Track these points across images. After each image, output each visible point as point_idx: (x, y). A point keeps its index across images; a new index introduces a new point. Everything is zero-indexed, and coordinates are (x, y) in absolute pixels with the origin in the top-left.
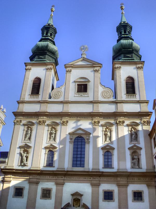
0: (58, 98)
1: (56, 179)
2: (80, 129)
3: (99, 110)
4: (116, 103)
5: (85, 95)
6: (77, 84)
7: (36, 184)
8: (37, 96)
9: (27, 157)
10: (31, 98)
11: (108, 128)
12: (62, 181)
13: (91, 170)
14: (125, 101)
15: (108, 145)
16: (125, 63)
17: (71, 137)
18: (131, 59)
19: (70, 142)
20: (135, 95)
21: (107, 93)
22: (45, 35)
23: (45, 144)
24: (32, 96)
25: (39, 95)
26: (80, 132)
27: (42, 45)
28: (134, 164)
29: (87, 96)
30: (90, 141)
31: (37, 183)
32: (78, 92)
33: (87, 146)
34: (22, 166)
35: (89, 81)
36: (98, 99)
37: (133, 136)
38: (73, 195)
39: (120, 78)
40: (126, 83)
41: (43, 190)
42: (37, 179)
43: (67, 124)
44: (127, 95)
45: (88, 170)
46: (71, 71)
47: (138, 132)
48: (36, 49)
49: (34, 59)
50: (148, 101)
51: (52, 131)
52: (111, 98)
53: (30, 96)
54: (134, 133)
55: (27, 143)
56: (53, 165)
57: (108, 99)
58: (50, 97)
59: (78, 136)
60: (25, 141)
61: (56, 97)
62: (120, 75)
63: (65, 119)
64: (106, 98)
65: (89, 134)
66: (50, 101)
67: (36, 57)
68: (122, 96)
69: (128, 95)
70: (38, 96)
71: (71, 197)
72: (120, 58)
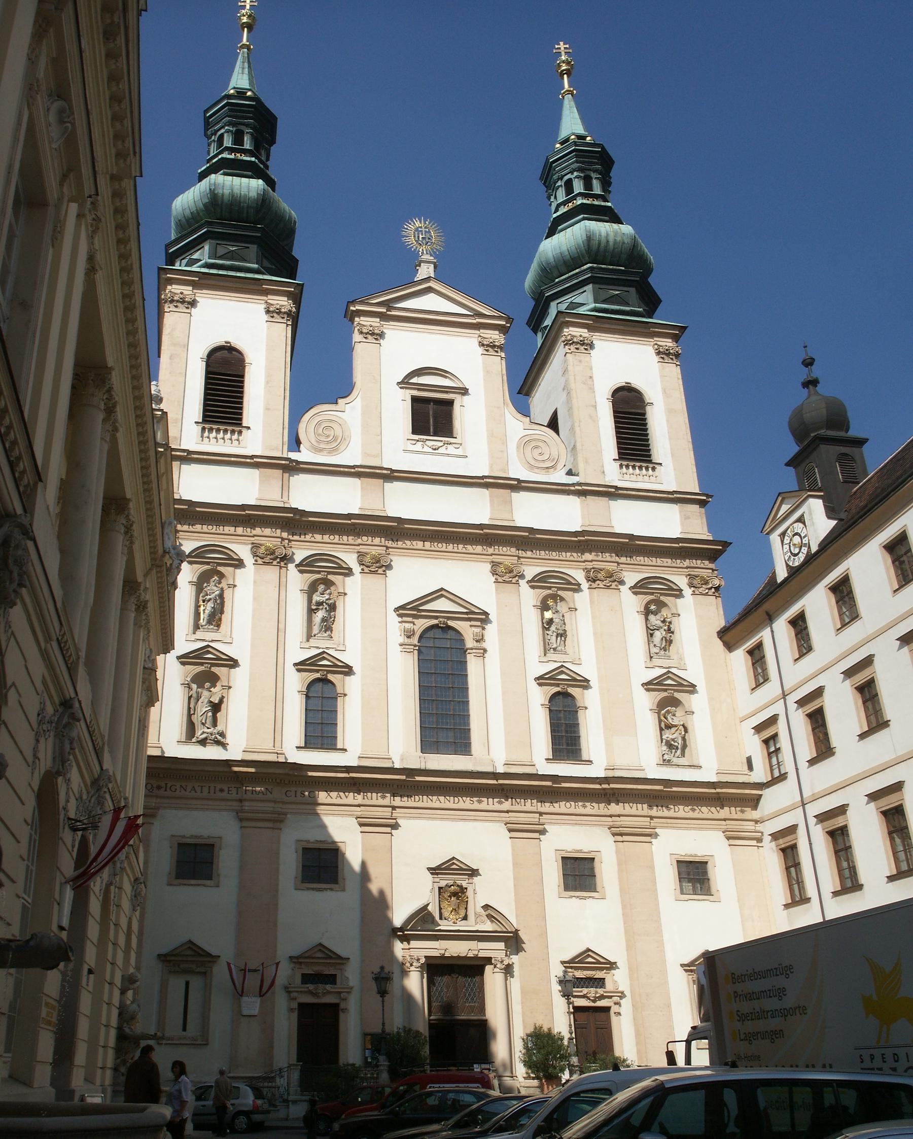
0: (333, 451)
1: (356, 803)
2: (442, 596)
3: (514, 518)
4: (583, 492)
5: (451, 450)
6: (408, 394)
7: (270, 825)
8: (233, 432)
9: (216, 708)
10: (206, 440)
11: (554, 597)
12: (387, 812)
13: (501, 769)
14: (616, 488)
15: (562, 666)
16: (607, 326)
17: (408, 626)
18: (628, 309)
19: (401, 645)
20: (654, 469)
21: (536, 447)
22: (228, 142)
23: (297, 651)
24: (211, 430)
25: (244, 431)
26: (442, 605)
27: (236, 191)
28: (670, 746)
29: (459, 452)
30: (484, 645)
31: (277, 821)
32: (414, 432)
33: (473, 665)
34: (203, 742)
35: (464, 391)
36: (505, 470)
37: (658, 635)
38: (435, 871)
39: (592, 389)
40: (615, 412)
41: (305, 850)
42: (275, 802)
43: (384, 571)
44: (621, 466)
45: (489, 769)
46: (381, 335)
47: (675, 620)
48: (201, 206)
49: (195, 256)
50: (708, 496)
51: (316, 598)
52: (556, 469)
53: (200, 428)
54: (659, 623)
55: (211, 644)
56: (336, 744)
57: (543, 472)
58: (295, 443)
59: (435, 622)
60: (200, 634)
61: (322, 446)
62: (591, 377)
63: (374, 546)
64: (536, 470)
65: (484, 617)
66: (298, 462)
67: (207, 248)
68: (603, 467)
69: (625, 463)
70: (240, 433)
71: (429, 876)
72: (579, 300)
